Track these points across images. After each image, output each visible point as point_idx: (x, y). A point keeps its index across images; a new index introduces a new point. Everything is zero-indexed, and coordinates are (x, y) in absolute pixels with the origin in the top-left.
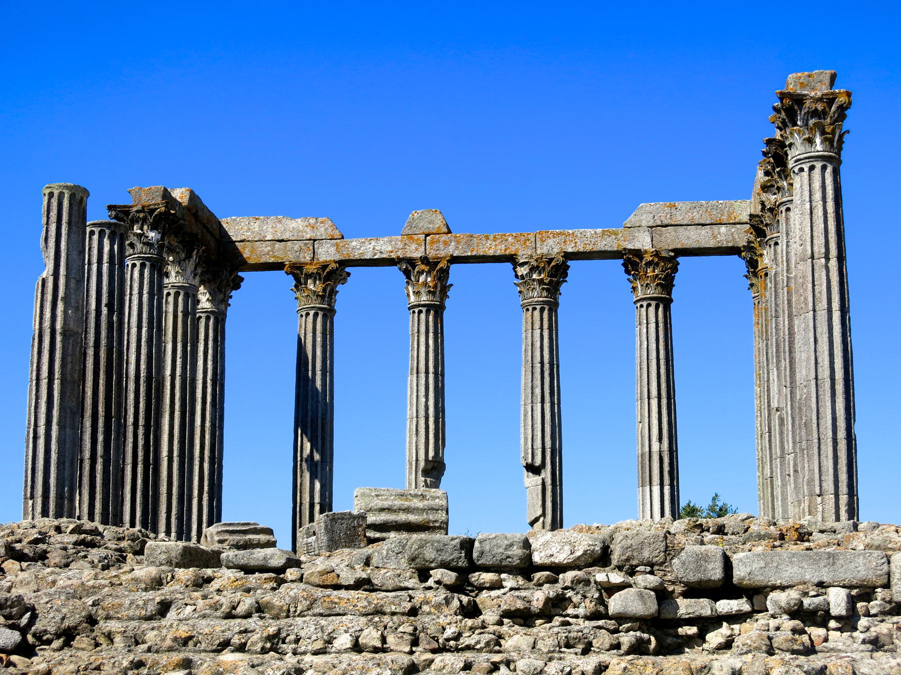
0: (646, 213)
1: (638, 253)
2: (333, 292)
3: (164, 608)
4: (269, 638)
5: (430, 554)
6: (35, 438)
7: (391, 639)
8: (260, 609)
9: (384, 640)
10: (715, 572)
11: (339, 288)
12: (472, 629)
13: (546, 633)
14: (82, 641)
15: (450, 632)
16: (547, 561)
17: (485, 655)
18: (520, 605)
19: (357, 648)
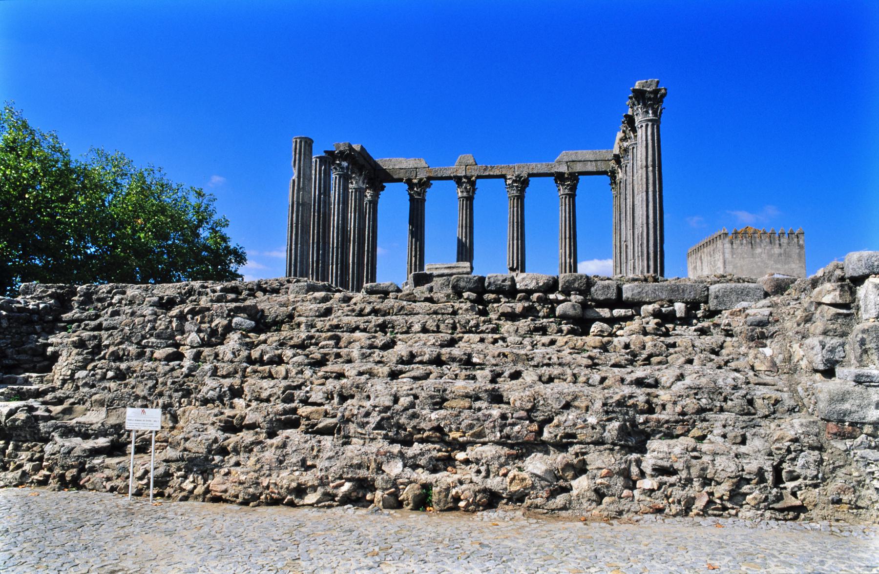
0: (566, 155)
1: (562, 174)
2: (425, 191)
3: (328, 312)
4: (378, 325)
5: (462, 284)
6: (291, 250)
7: (442, 326)
8: (375, 312)
9: (438, 326)
10: (612, 295)
11: (427, 190)
12: (484, 322)
13: (524, 324)
14: (285, 327)
15: (472, 323)
16: (523, 288)
17: (490, 335)
18: (509, 310)
19: (424, 330)
